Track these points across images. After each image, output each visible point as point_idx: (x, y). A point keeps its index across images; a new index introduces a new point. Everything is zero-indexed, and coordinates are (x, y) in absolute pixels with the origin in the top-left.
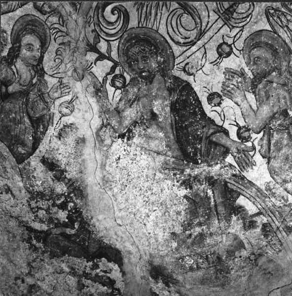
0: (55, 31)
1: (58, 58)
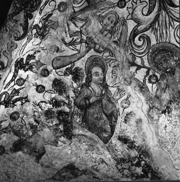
0: (109, 60)
1: (114, 76)
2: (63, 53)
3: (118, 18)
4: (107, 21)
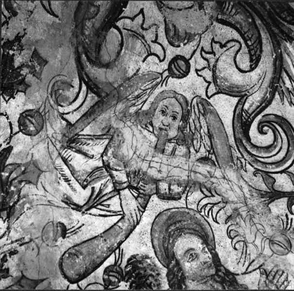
0: (207, 209)
1: (238, 242)
2: (80, 233)
3: (185, 103)
4: (162, 118)
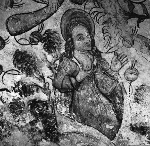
0: (95, 14)
2: (21, 8)
